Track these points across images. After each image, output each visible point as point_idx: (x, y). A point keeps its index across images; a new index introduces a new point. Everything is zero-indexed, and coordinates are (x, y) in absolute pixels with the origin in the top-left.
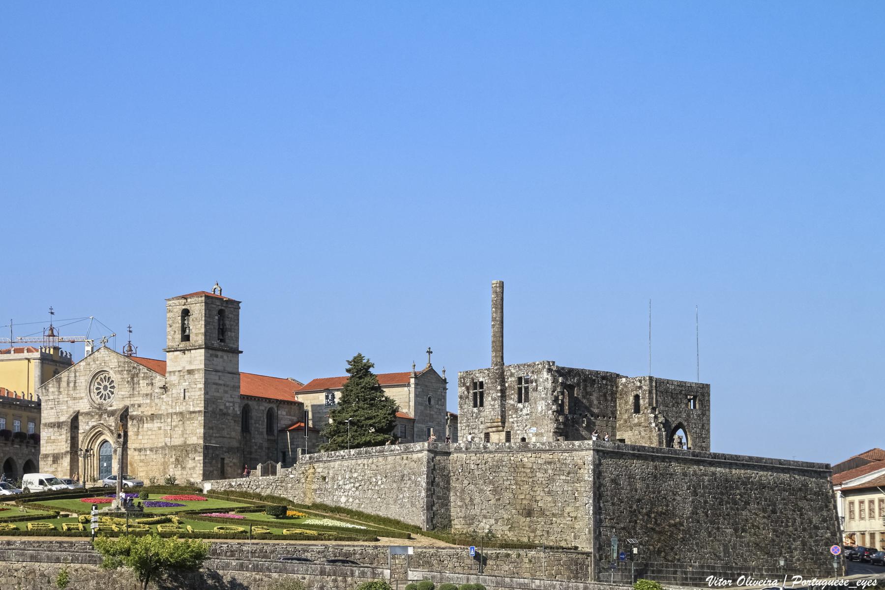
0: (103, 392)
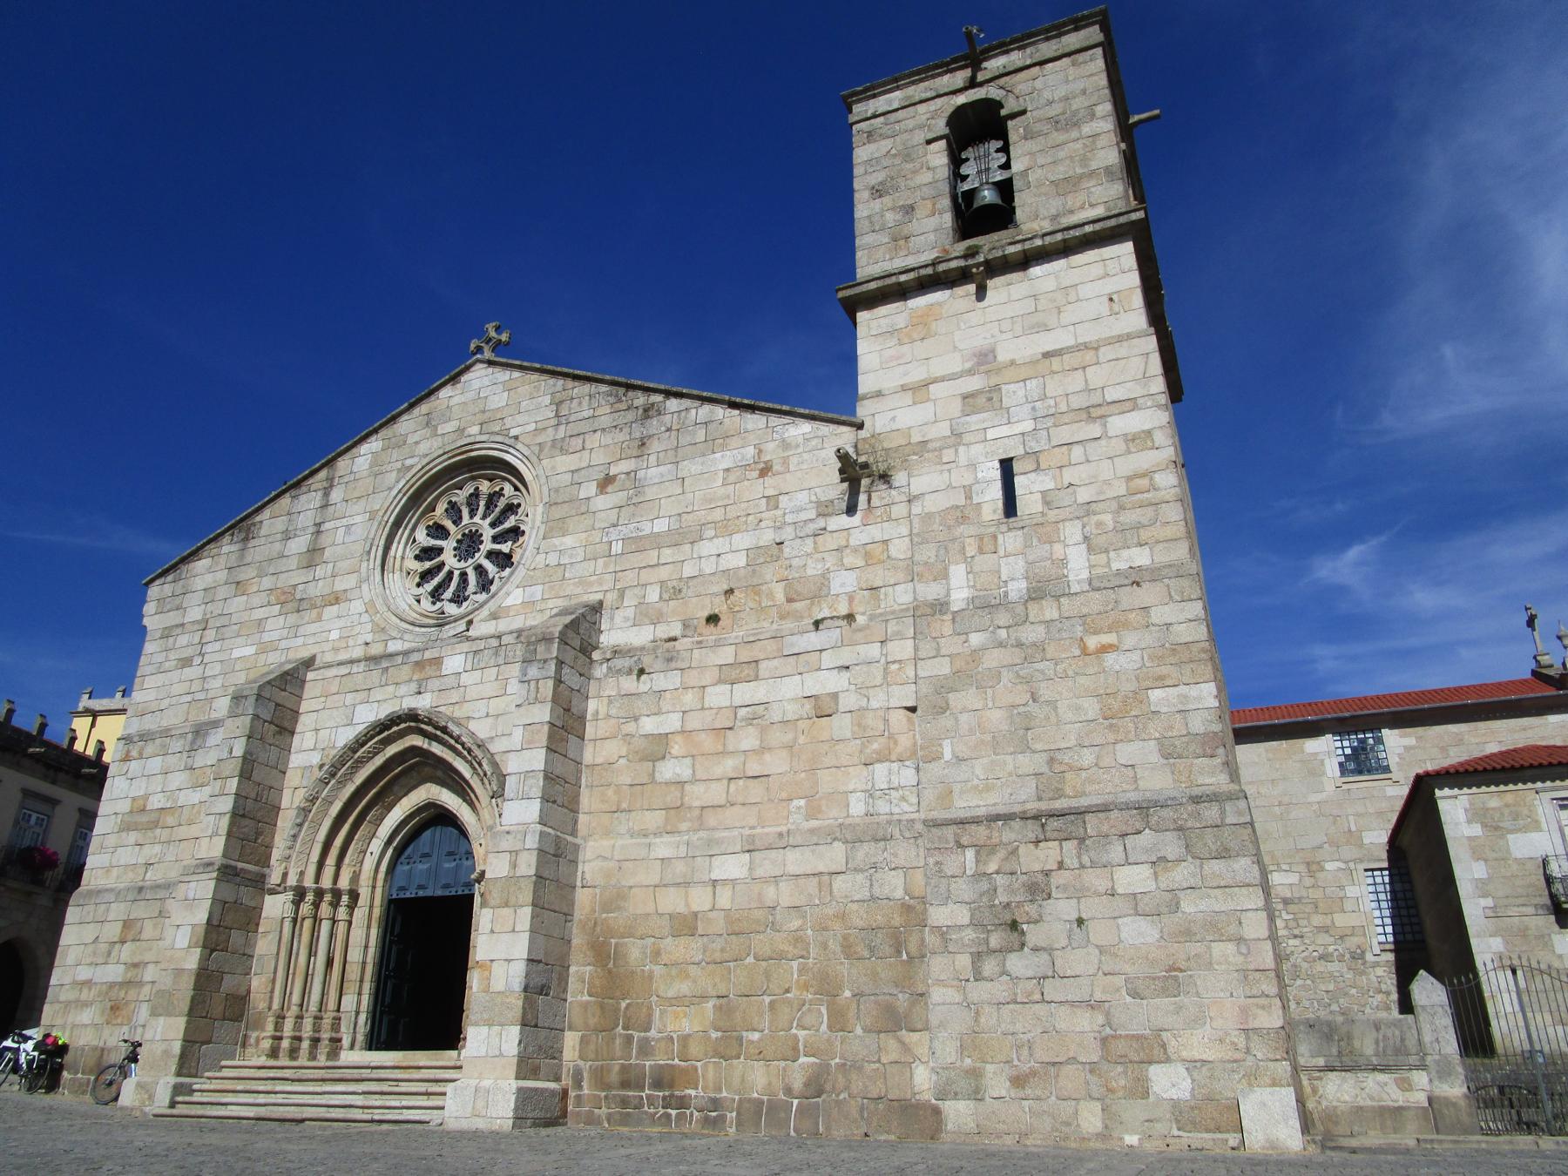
0: (449, 559)
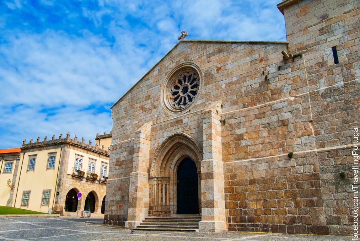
0: (181, 95)
